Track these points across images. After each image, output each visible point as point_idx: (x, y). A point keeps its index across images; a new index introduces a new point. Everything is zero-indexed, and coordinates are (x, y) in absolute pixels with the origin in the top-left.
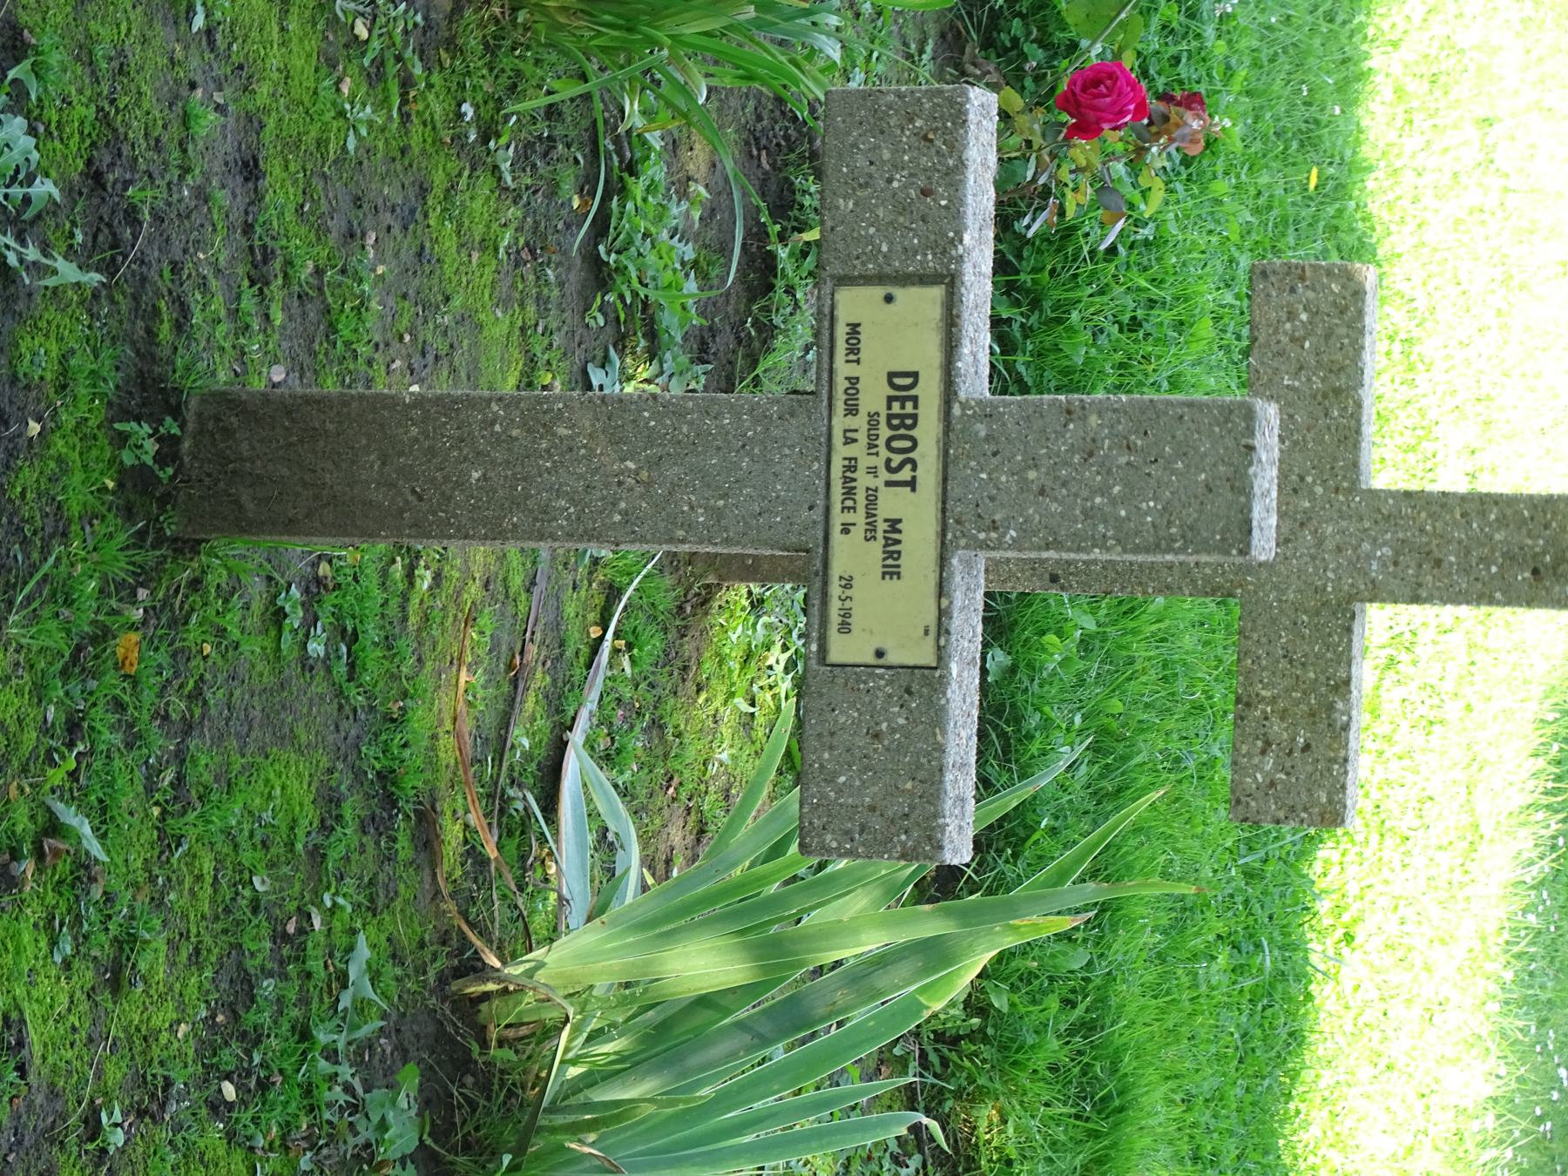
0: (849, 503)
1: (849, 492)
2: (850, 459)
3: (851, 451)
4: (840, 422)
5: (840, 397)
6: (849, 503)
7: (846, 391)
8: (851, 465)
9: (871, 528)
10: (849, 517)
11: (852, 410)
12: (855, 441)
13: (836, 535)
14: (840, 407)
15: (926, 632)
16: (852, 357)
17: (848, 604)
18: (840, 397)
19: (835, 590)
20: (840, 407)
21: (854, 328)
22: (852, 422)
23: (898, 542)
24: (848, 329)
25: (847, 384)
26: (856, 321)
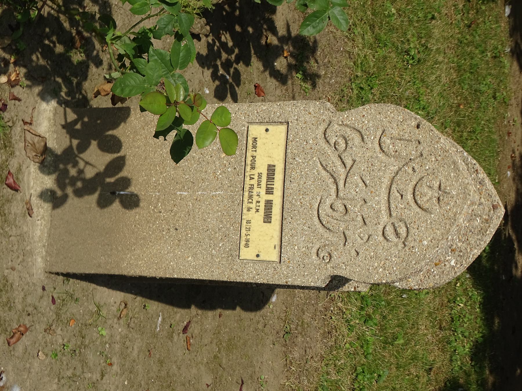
0: (250, 201)
1: (250, 197)
2: (251, 185)
6: (250, 201)
8: (252, 187)
9: (257, 211)
10: (251, 205)
11: (253, 168)
12: (253, 178)
13: (245, 211)
15: (275, 248)
17: (248, 237)
18: (249, 162)
19: (244, 232)
21: (255, 139)
25: (252, 158)
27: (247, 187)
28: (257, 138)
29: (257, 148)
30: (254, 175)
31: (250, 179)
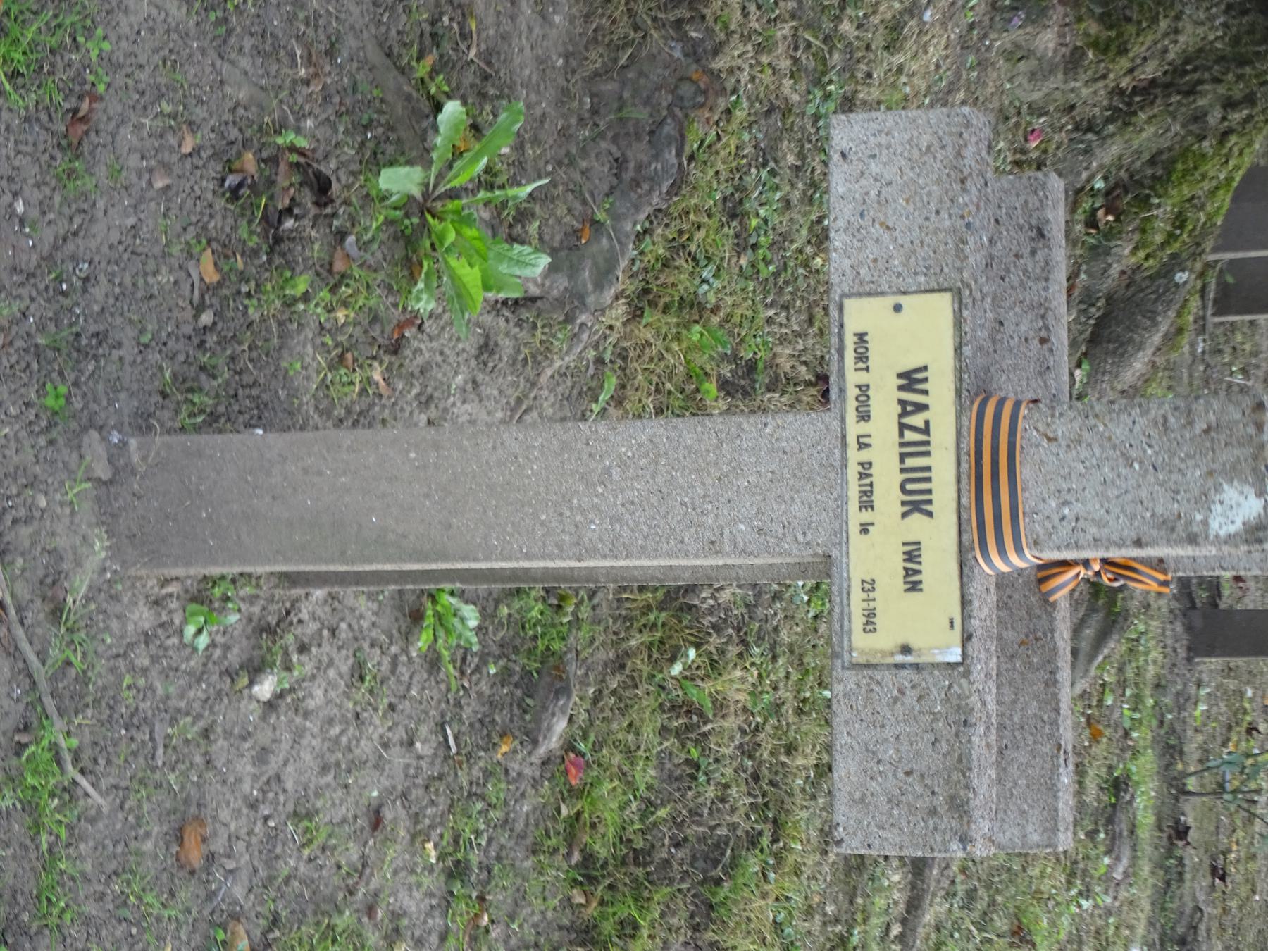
3: (865, 455)
4: (854, 429)
5: (851, 405)
7: (857, 399)
11: (864, 417)
12: (868, 445)
14: (851, 416)
16: (861, 365)
17: (872, 604)
20: (851, 416)
21: (861, 337)
22: (863, 428)
23: (918, 572)
24: (855, 339)
25: (857, 392)
26: (860, 331)
27: (853, 471)
28: (866, 334)
29: (870, 363)
30: (869, 436)
31: (860, 448)
